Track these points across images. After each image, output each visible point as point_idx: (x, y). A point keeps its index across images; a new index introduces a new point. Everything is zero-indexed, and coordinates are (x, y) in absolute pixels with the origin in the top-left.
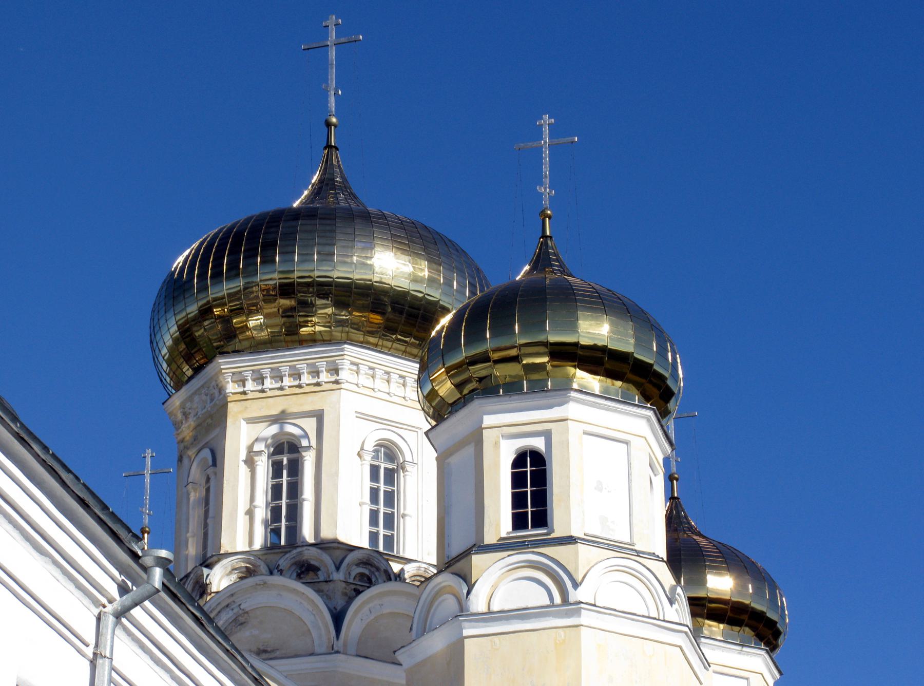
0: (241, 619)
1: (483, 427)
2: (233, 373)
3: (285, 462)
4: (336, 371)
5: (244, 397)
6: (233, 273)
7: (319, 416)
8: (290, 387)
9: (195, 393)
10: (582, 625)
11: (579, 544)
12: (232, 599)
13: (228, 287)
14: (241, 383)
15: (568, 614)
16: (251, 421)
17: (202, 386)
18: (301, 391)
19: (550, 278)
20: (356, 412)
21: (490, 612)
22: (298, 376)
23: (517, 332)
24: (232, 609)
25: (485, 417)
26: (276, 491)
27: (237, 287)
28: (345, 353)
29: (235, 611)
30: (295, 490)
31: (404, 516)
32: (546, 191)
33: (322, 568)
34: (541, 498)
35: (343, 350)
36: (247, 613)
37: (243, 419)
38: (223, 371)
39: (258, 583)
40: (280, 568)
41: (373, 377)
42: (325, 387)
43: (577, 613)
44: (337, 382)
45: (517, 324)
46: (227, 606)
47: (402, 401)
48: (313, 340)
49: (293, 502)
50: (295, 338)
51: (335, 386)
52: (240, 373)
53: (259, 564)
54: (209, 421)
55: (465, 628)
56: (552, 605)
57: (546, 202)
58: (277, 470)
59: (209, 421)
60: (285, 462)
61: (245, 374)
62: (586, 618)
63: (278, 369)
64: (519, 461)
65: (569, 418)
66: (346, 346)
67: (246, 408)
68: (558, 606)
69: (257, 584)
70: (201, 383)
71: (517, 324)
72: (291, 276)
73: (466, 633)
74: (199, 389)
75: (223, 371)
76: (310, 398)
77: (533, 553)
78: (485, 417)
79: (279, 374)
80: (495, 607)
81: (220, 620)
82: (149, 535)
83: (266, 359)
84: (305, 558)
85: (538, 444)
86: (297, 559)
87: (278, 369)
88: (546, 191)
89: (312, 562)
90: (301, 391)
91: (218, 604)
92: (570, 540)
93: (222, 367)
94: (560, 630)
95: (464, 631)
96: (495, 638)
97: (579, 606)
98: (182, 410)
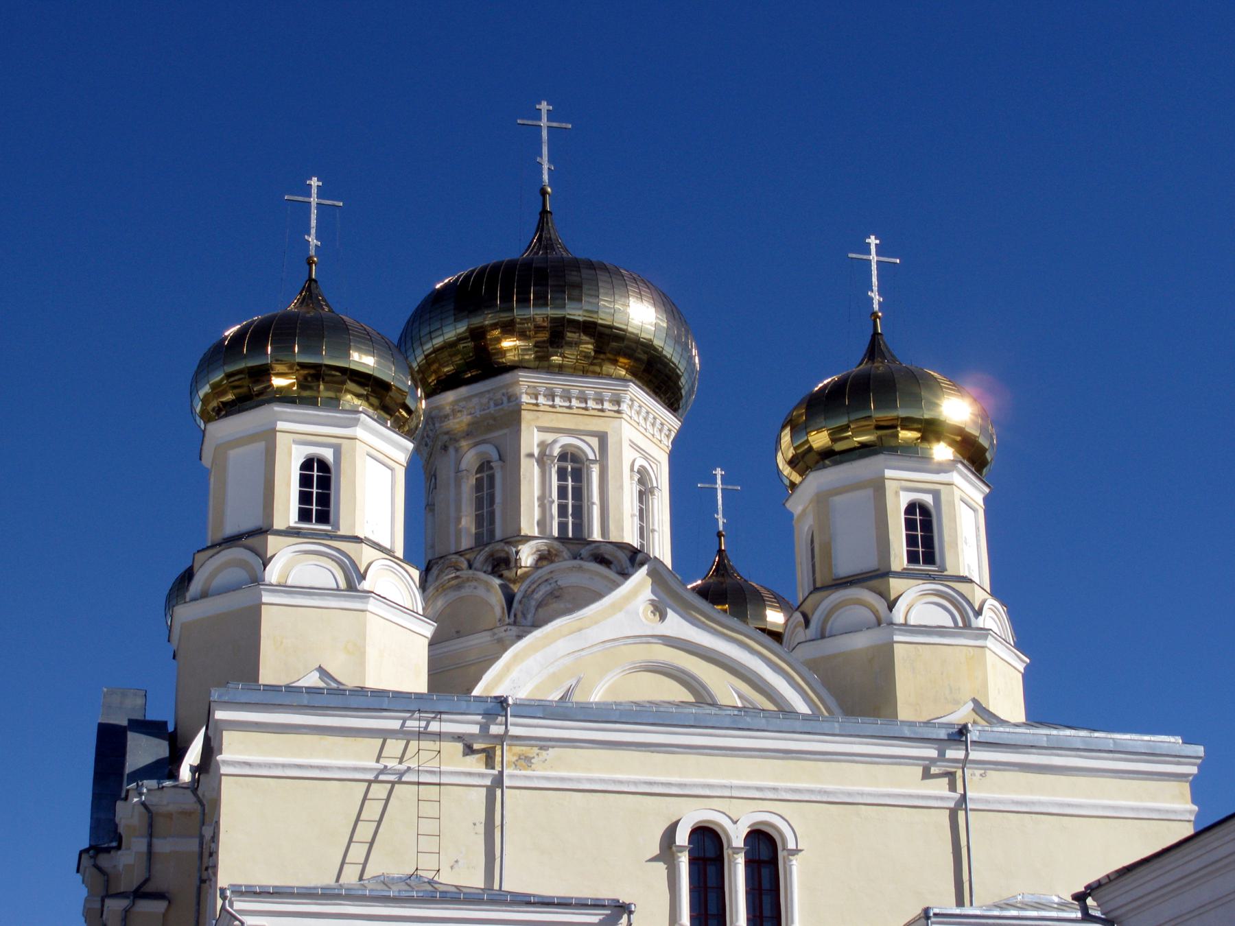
0: (557, 594)
1: (277, 429)
2: (529, 386)
3: (569, 469)
4: (618, 402)
5: (536, 408)
6: (541, 302)
7: (603, 438)
8: (577, 408)
9: (476, 395)
10: (369, 611)
11: (363, 544)
12: (550, 576)
13: (535, 313)
14: (550, 398)
15: (977, 637)
16: (542, 429)
17: (488, 391)
18: (587, 413)
19: (880, 367)
20: (630, 440)
21: (906, 624)
22: (601, 401)
23: (269, 353)
24: (550, 584)
25: (278, 423)
26: (562, 492)
27: (545, 314)
28: (630, 389)
29: (552, 585)
30: (578, 494)
31: (653, 531)
32: (876, 298)
33: (615, 562)
34: (929, 542)
35: (628, 386)
36: (561, 589)
37: (537, 427)
38: (521, 383)
39: (575, 566)
40: (582, 556)
41: (638, 413)
42: (608, 414)
43: (985, 637)
44: (618, 412)
45: (296, 346)
46: (546, 580)
47: (651, 437)
48: (560, 370)
49: (577, 503)
50: (546, 364)
51: (616, 415)
52: (535, 387)
53: (561, 550)
54: (491, 422)
55: (896, 635)
56: (338, 589)
57: (876, 307)
58: (562, 474)
59: (491, 422)
60: (569, 469)
61: (540, 389)
62: (372, 605)
63: (568, 391)
64: (307, 465)
65: (358, 438)
66: (631, 384)
67: (538, 418)
68: (960, 628)
69: (573, 567)
70: (489, 388)
71: (296, 346)
72: (595, 316)
73: (896, 638)
74: (481, 393)
75: (521, 383)
76: (595, 420)
77: (942, 584)
78: (278, 423)
79: (568, 396)
80: (912, 621)
81: (540, 590)
82: (717, 531)
83: (580, 382)
84: (601, 552)
85: (328, 454)
86: (595, 551)
87: (568, 391)
88: (876, 298)
89: (606, 556)
90: (587, 413)
91: (540, 578)
92: (356, 539)
93: (520, 379)
94: (970, 649)
95: (894, 637)
96: (919, 647)
97: (370, 594)
98: (451, 407)
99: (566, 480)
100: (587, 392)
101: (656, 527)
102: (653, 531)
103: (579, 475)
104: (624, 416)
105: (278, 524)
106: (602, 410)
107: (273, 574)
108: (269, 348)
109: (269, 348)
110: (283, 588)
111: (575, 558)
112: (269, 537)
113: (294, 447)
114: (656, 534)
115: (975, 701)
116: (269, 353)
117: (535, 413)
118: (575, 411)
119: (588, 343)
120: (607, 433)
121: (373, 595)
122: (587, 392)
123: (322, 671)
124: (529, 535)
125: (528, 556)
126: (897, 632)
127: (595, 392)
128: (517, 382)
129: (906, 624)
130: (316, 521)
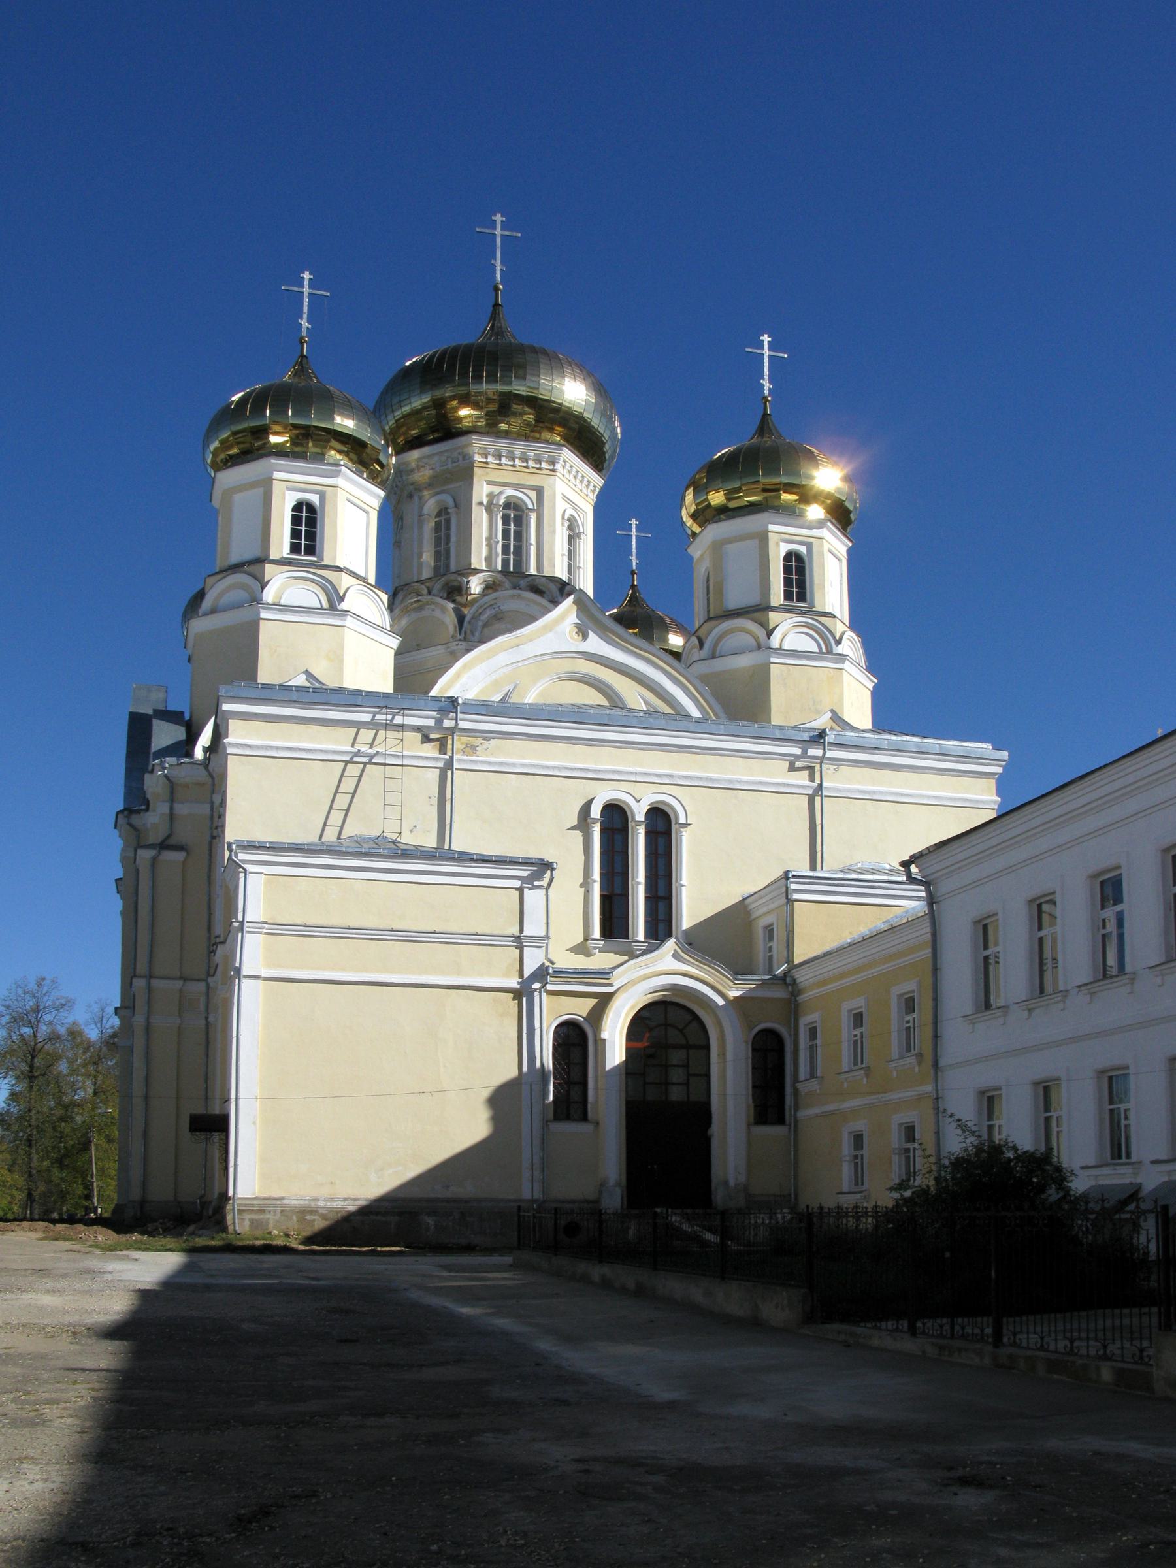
2: (480, 448)
3: (512, 516)
5: (485, 465)
7: (540, 491)
16: (490, 483)
17: (446, 451)
19: (768, 441)
21: (780, 649)
23: (268, 415)
26: (506, 534)
30: (519, 536)
31: (579, 568)
32: (767, 385)
34: (801, 584)
35: (562, 450)
43: (843, 661)
48: (506, 435)
49: (517, 544)
50: (495, 429)
52: (485, 448)
57: (766, 392)
60: (512, 516)
61: (489, 450)
62: (349, 621)
64: (298, 507)
67: (487, 473)
68: (824, 653)
72: (535, 391)
73: (773, 660)
74: (442, 452)
80: (785, 647)
85: (315, 499)
87: (512, 452)
88: (767, 385)
89: (540, 587)
92: (337, 569)
99: (509, 525)
101: (581, 565)
102: (579, 568)
103: (520, 521)
104: (558, 474)
105: (274, 555)
106: (540, 469)
107: (269, 595)
108: (268, 411)
109: (268, 411)
110: (278, 607)
111: (515, 588)
112: (267, 565)
113: (287, 492)
114: (581, 570)
115: (832, 711)
116: (268, 415)
118: (518, 469)
119: (529, 414)
120: (543, 487)
123: (307, 673)
125: (477, 586)
126: (773, 655)
128: (471, 444)
129: (780, 649)
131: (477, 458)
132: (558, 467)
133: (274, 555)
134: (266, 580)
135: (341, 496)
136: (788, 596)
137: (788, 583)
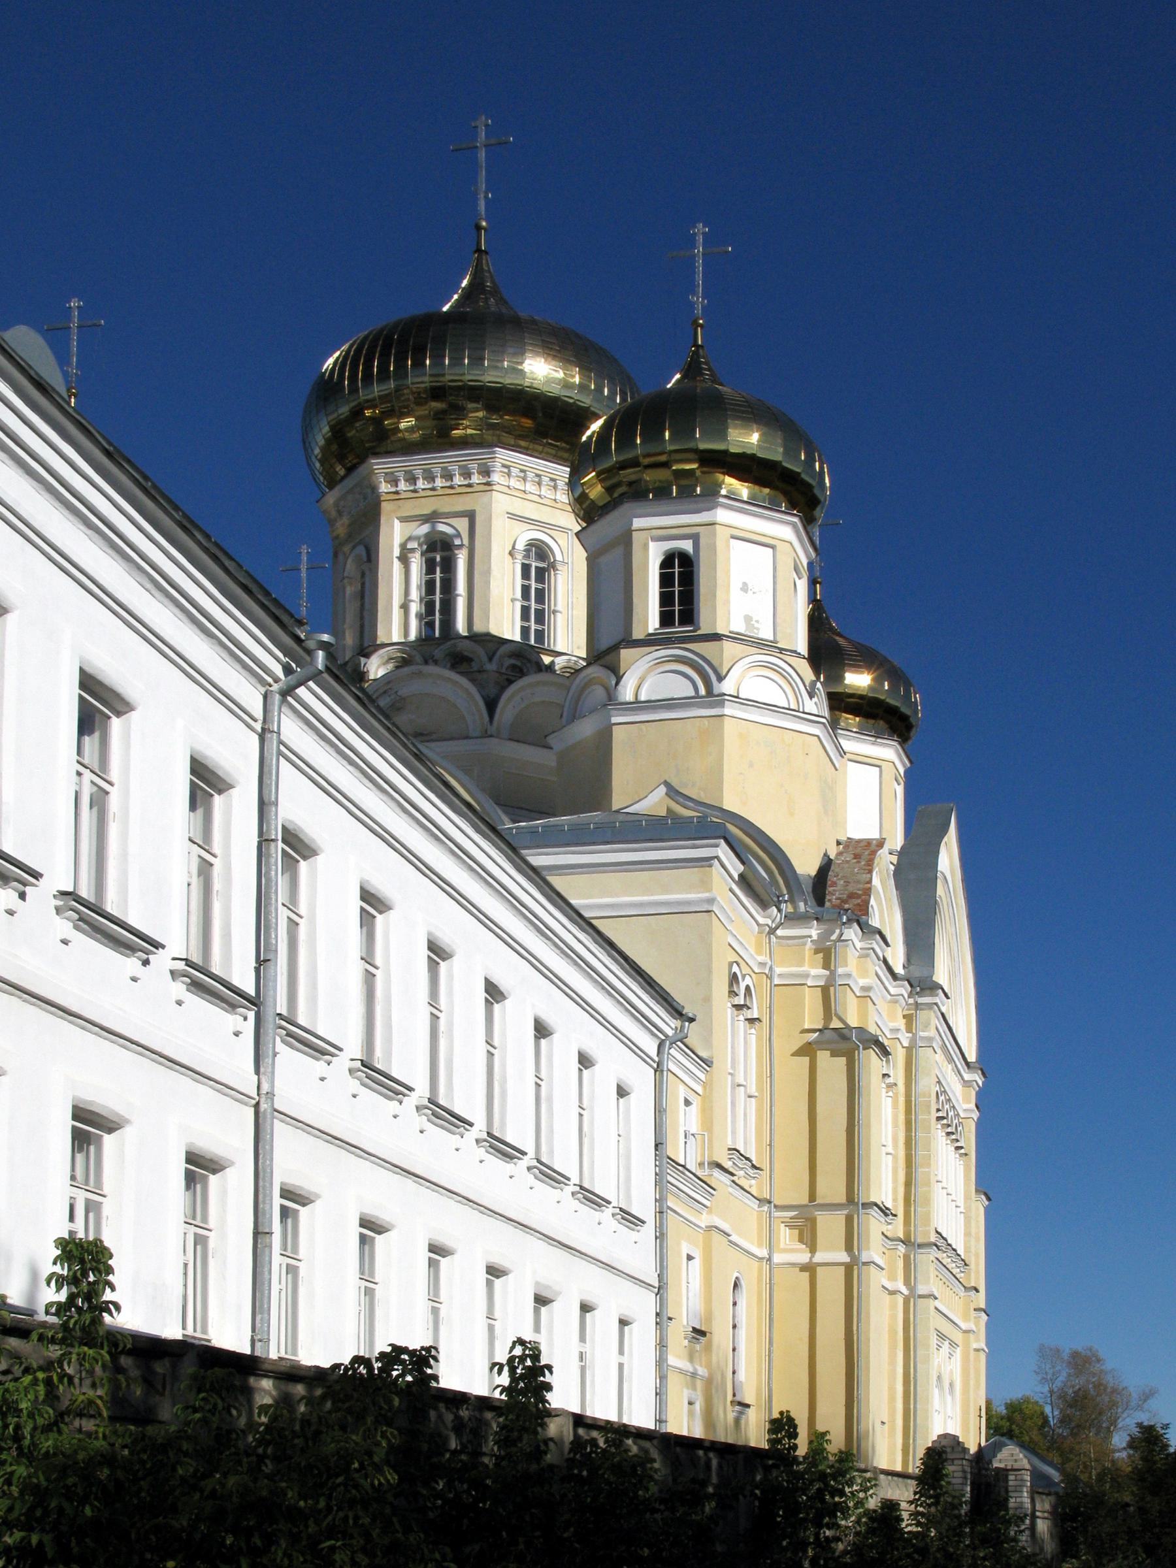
1: (633, 528)
3: (438, 559)
4: (486, 472)
7: (471, 516)
8: (442, 487)
14: (394, 483)
15: (711, 705)
20: (508, 513)
21: (637, 702)
23: (667, 438)
24: (389, 696)
25: (635, 520)
26: (430, 587)
28: (497, 455)
29: (392, 697)
30: (448, 586)
31: (555, 612)
35: (494, 453)
36: (404, 699)
37: (397, 518)
38: (376, 471)
43: (721, 704)
46: (385, 692)
48: (464, 443)
52: (392, 473)
58: (430, 567)
60: (438, 559)
62: (728, 710)
63: (431, 472)
68: (702, 697)
73: (614, 720)
75: (376, 471)
76: (461, 498)
78: (635, 520)
80: (643, 697)
85: (687, 546)
89: (466, 653)
91: (377, 690)
92: (716, 637)
96: (642, 726)
99: (435, 573)
100: (450, 468)
101: (559, 608)
102: (555, 612)
103: (449, 566)
104: (494, 487)
105: (637, 634)
106: (470, 486)
107: (627, 692)
108: (667, 434)
109: (667, 434)
110: (638, 705)
111: (426, 662)
112: (622, 650)
113: (652, 545)
114: (559, 615)
115: (667, 784)
116: (667, 438)
117: (396, 502)
118: (440, 492)
119: (477, 410)
120: (475, 510)
121: (727, 697)
122: (450, 468)
123: (673, 792)
124: (386, 642)
125: (379, 667)
126: (613, 712)
127: (478, 464)
128: (372, 472)
129: (637, 702)
130: (679, 624)
131: (384, 487)
132: (496, 477)
133: (637, 634)
134: (621, 674)
135: (721, 534)
136: (666, 619)
137: (666, 599)
